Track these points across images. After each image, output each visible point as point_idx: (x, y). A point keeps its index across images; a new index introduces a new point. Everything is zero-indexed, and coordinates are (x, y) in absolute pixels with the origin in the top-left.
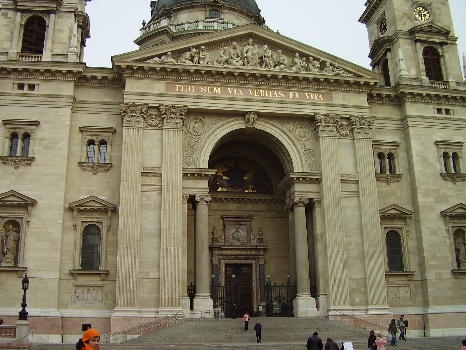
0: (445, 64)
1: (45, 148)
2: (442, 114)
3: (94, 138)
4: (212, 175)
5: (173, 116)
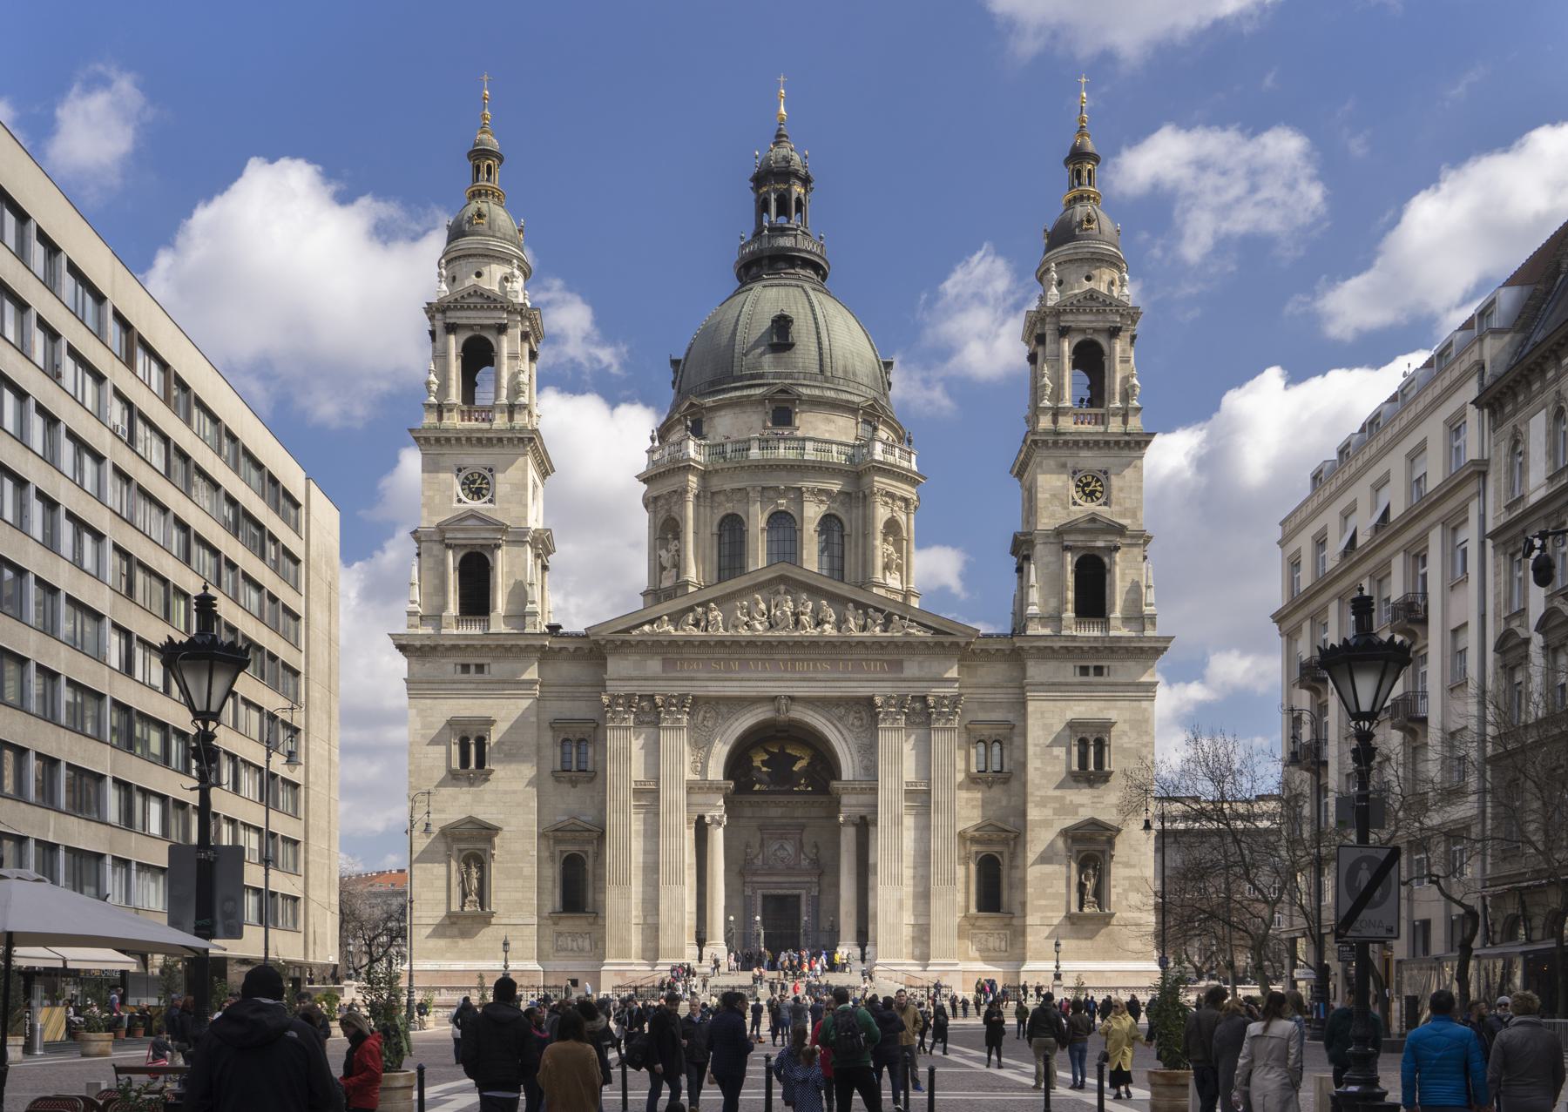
0: (1110, 585)
1: (505, 755)
2: (1087, 674)
3: (571, 737)
4: (727, 788)
5: (674, 709)
